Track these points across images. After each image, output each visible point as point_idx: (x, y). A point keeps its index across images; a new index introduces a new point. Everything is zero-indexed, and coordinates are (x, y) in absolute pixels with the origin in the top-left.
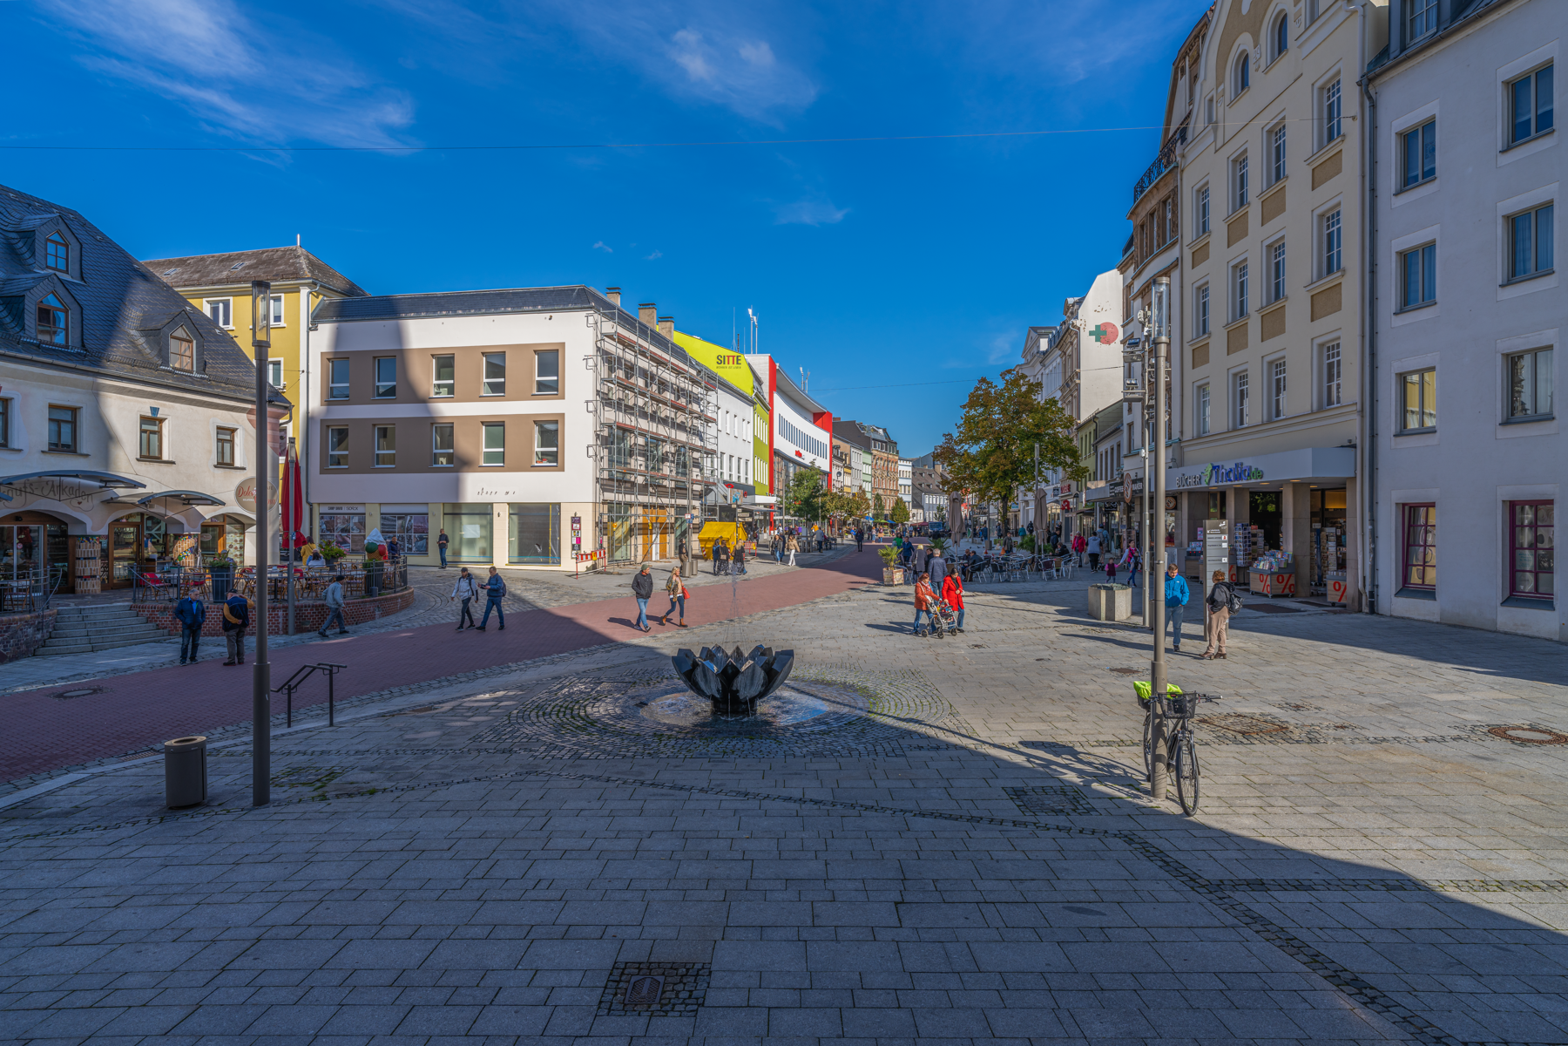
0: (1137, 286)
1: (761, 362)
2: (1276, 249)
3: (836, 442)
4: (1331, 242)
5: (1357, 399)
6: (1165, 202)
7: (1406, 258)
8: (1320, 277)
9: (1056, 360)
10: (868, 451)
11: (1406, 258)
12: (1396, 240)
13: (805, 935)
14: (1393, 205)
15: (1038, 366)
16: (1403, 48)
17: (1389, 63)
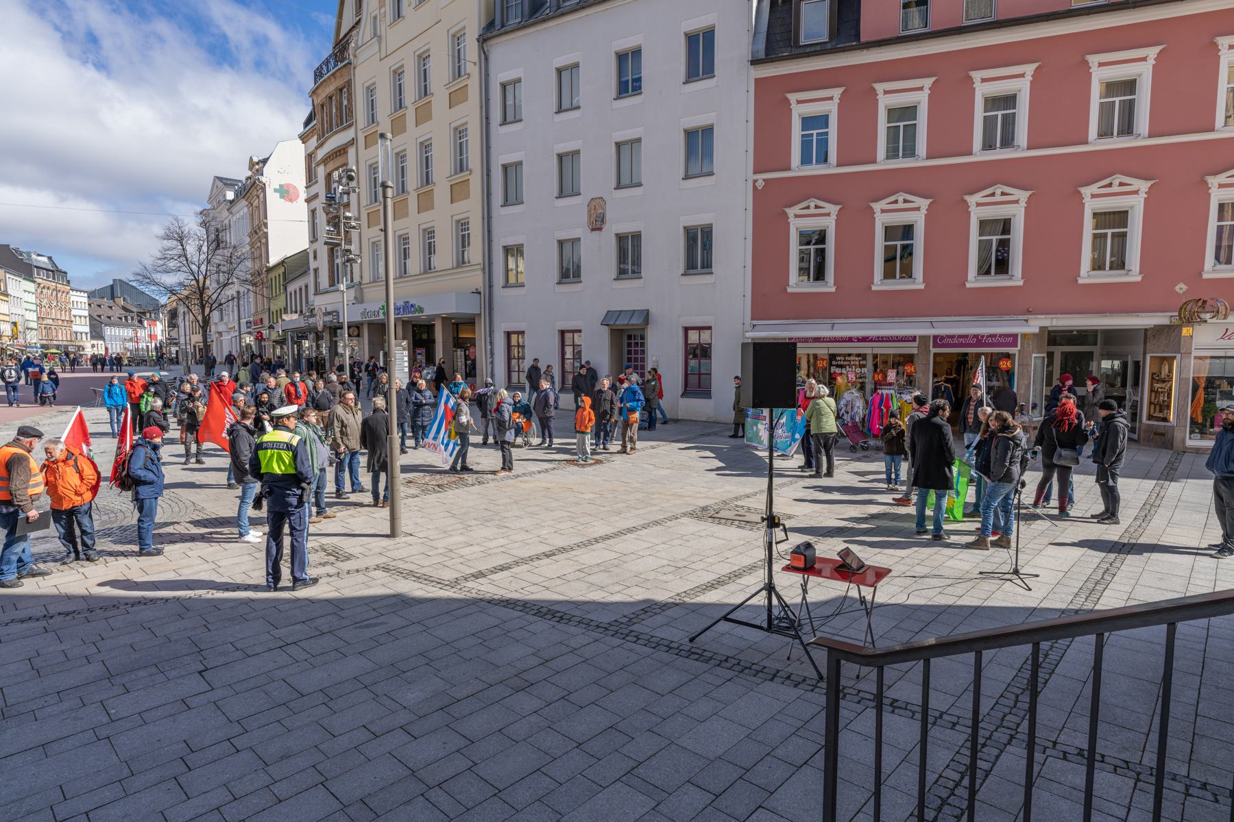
0: (321, 154)
2: (425, 147)
4: (461, 149)
5: (481, 261)
6: (341, 90)
7: (505, 168)
8: (456, 173)
9: (242, 209)
10: (29, 277)
11: (505, 168)
12: (501, 157)
13: (103, 733)
14: (500, 133)
15: (225, 213)
16: (503, 26)
17: (495, 33)
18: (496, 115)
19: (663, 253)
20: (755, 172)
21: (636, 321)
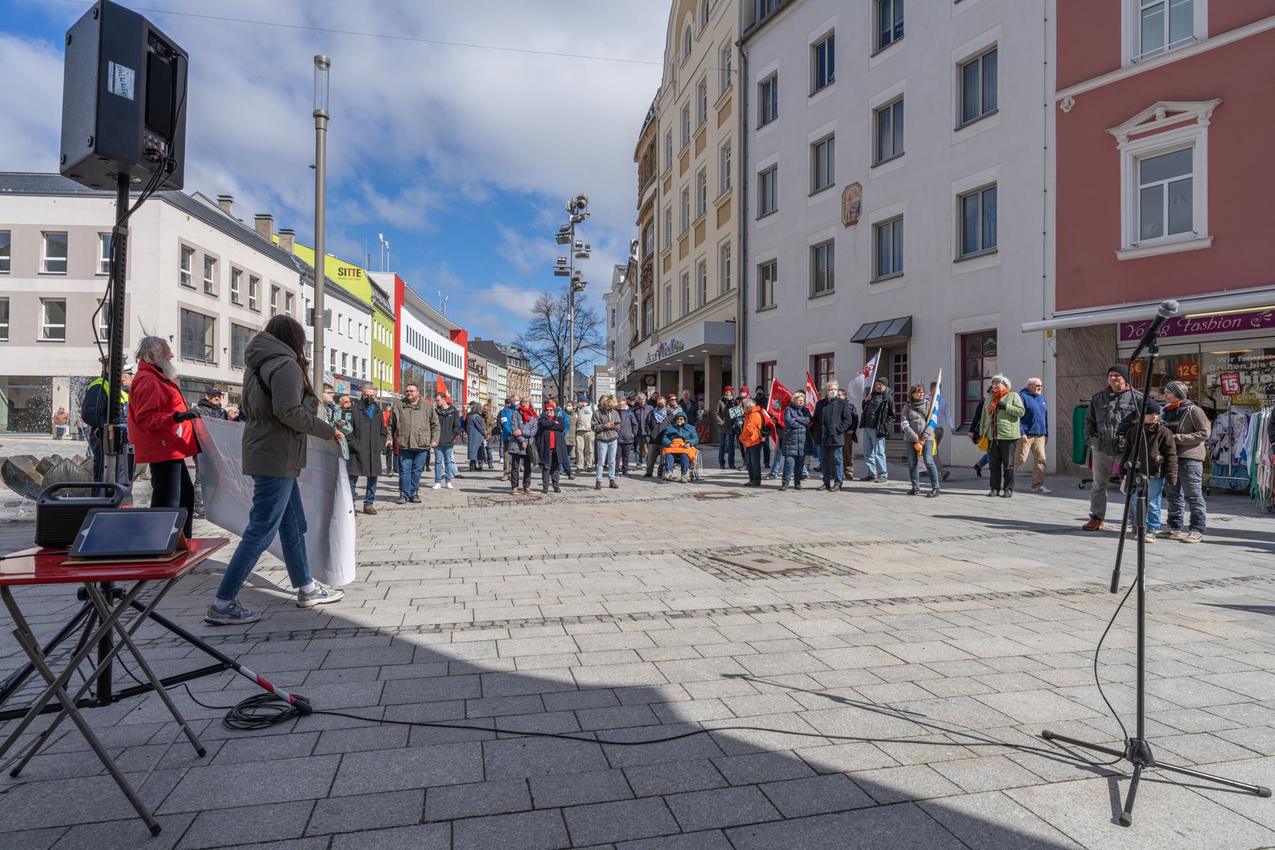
1: (387, 281)
2: (702, 176)
3: (472, 356)
10: (504, 366)
12: (758, 165)
18: (754, 118)
19: (930, 236)
20: (1060, 87)
21: (893, 331)
